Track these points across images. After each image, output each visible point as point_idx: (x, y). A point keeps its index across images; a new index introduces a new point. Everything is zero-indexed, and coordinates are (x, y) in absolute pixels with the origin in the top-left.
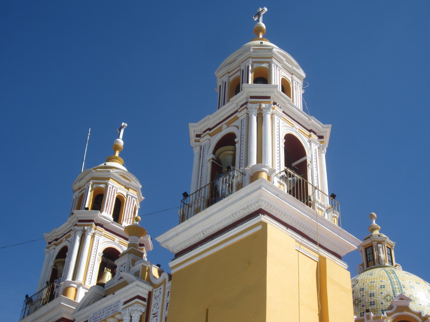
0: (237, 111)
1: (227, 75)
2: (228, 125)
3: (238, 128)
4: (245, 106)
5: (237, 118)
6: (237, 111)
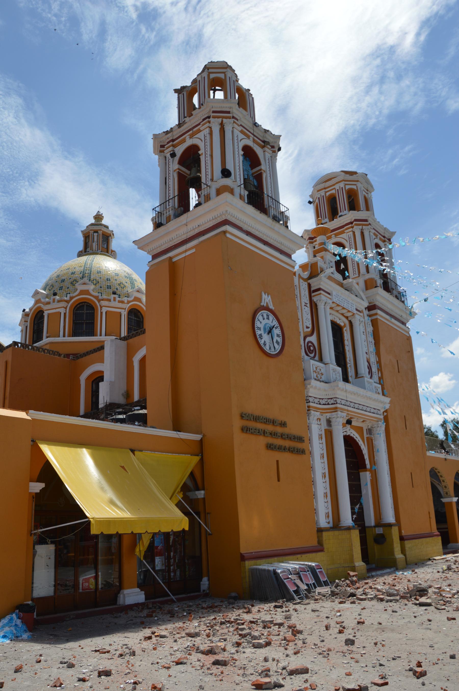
0: (199, 124)
1: (324, 190)
2: (191, 137)
3: (202, 141)
4: (207, 120)
5: (199, 131)
6: (199, 124)
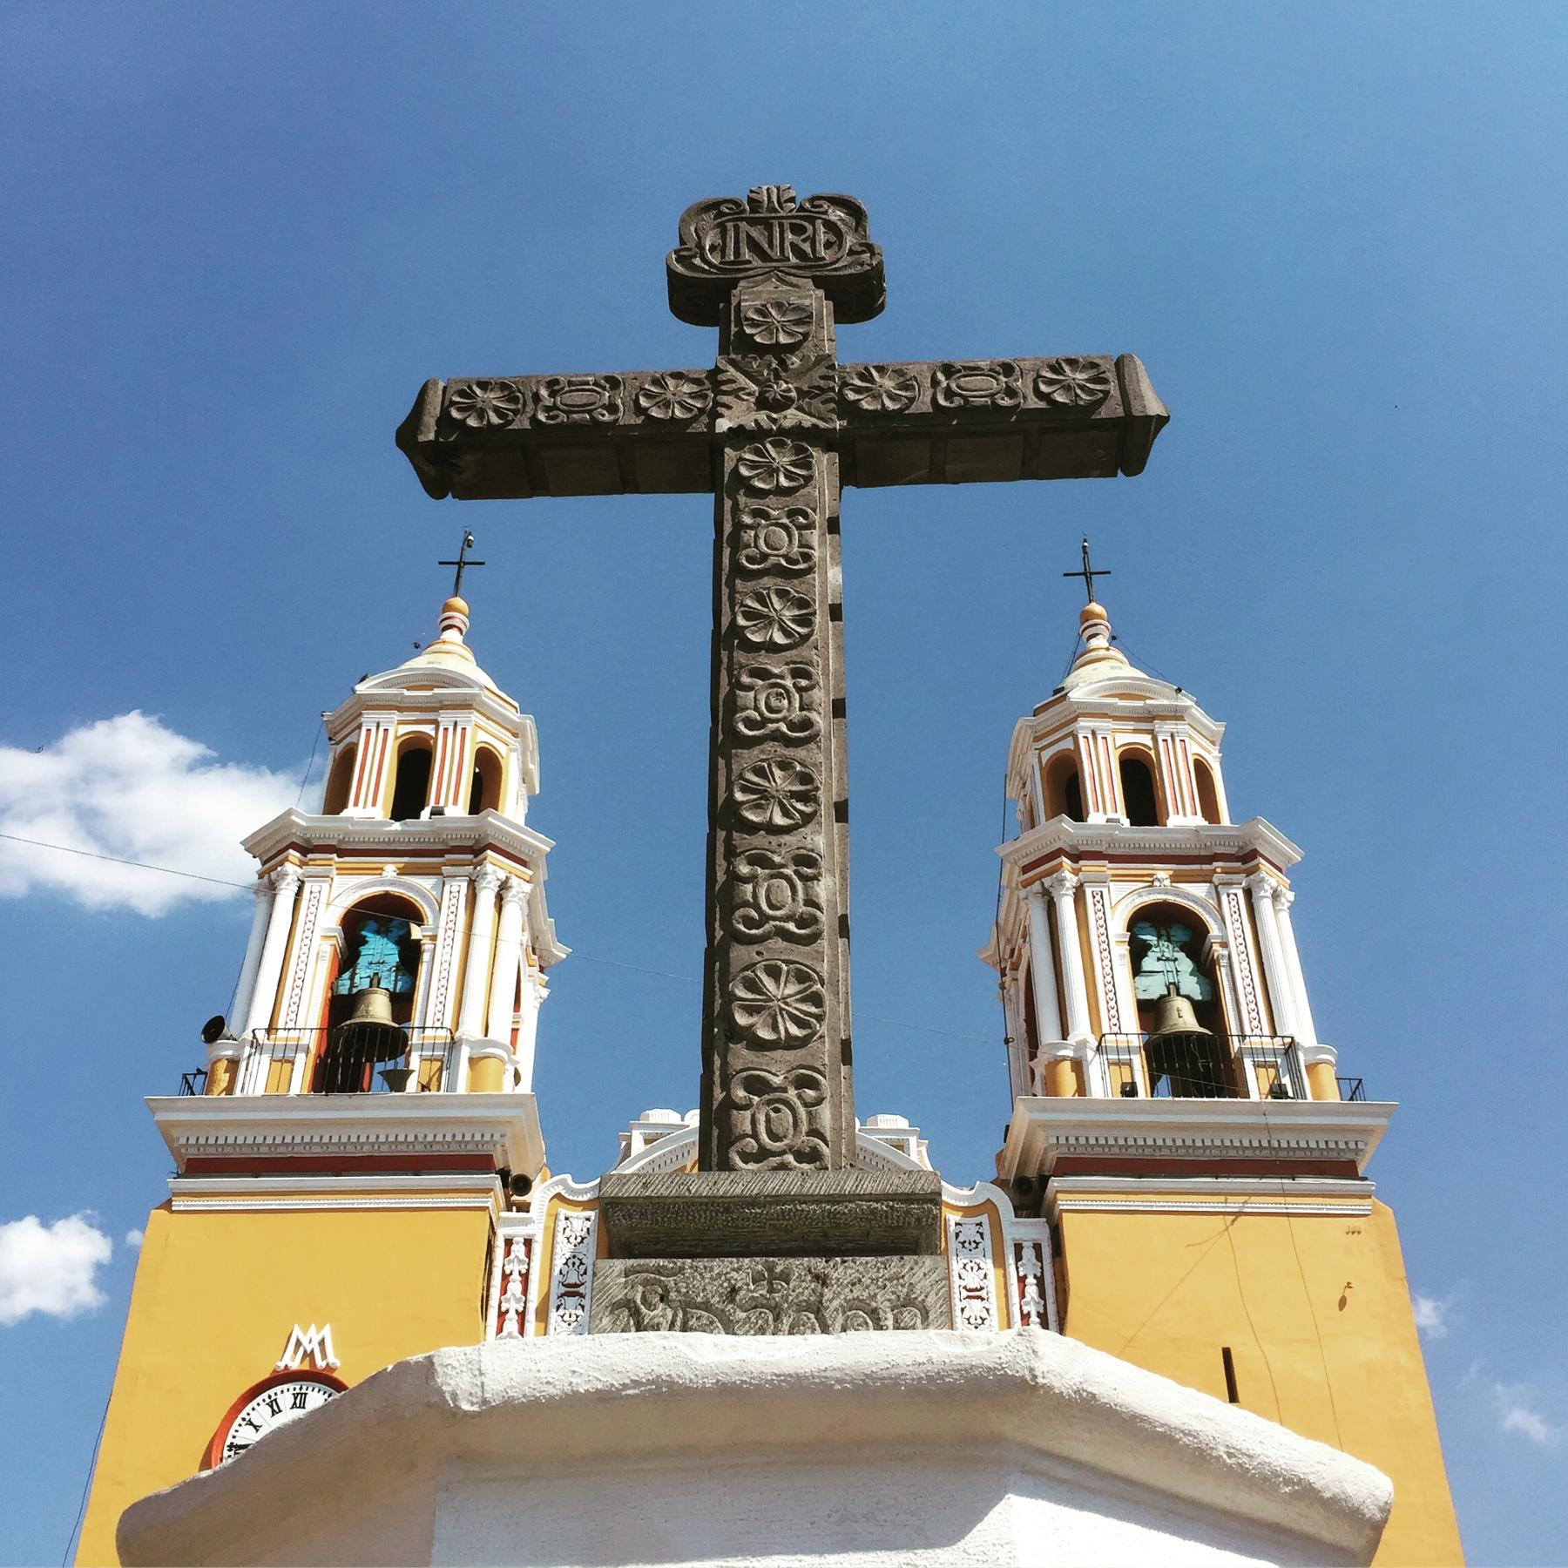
6: (441, 853)
